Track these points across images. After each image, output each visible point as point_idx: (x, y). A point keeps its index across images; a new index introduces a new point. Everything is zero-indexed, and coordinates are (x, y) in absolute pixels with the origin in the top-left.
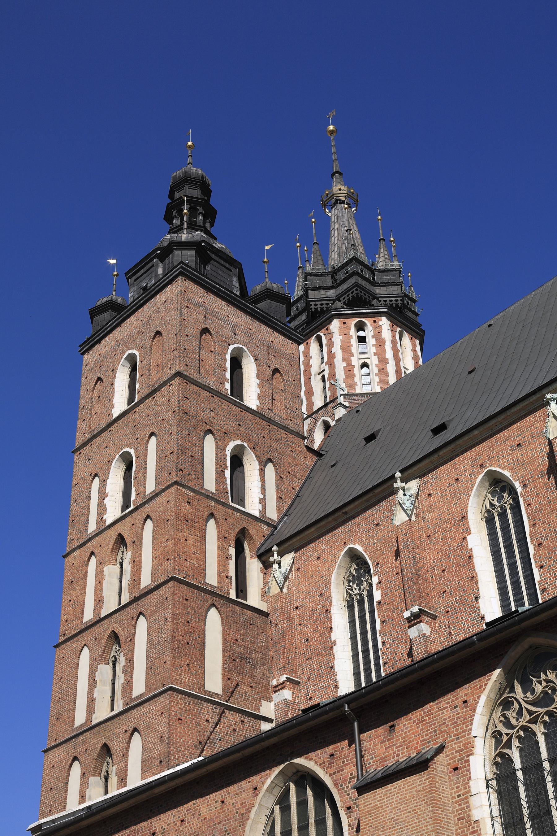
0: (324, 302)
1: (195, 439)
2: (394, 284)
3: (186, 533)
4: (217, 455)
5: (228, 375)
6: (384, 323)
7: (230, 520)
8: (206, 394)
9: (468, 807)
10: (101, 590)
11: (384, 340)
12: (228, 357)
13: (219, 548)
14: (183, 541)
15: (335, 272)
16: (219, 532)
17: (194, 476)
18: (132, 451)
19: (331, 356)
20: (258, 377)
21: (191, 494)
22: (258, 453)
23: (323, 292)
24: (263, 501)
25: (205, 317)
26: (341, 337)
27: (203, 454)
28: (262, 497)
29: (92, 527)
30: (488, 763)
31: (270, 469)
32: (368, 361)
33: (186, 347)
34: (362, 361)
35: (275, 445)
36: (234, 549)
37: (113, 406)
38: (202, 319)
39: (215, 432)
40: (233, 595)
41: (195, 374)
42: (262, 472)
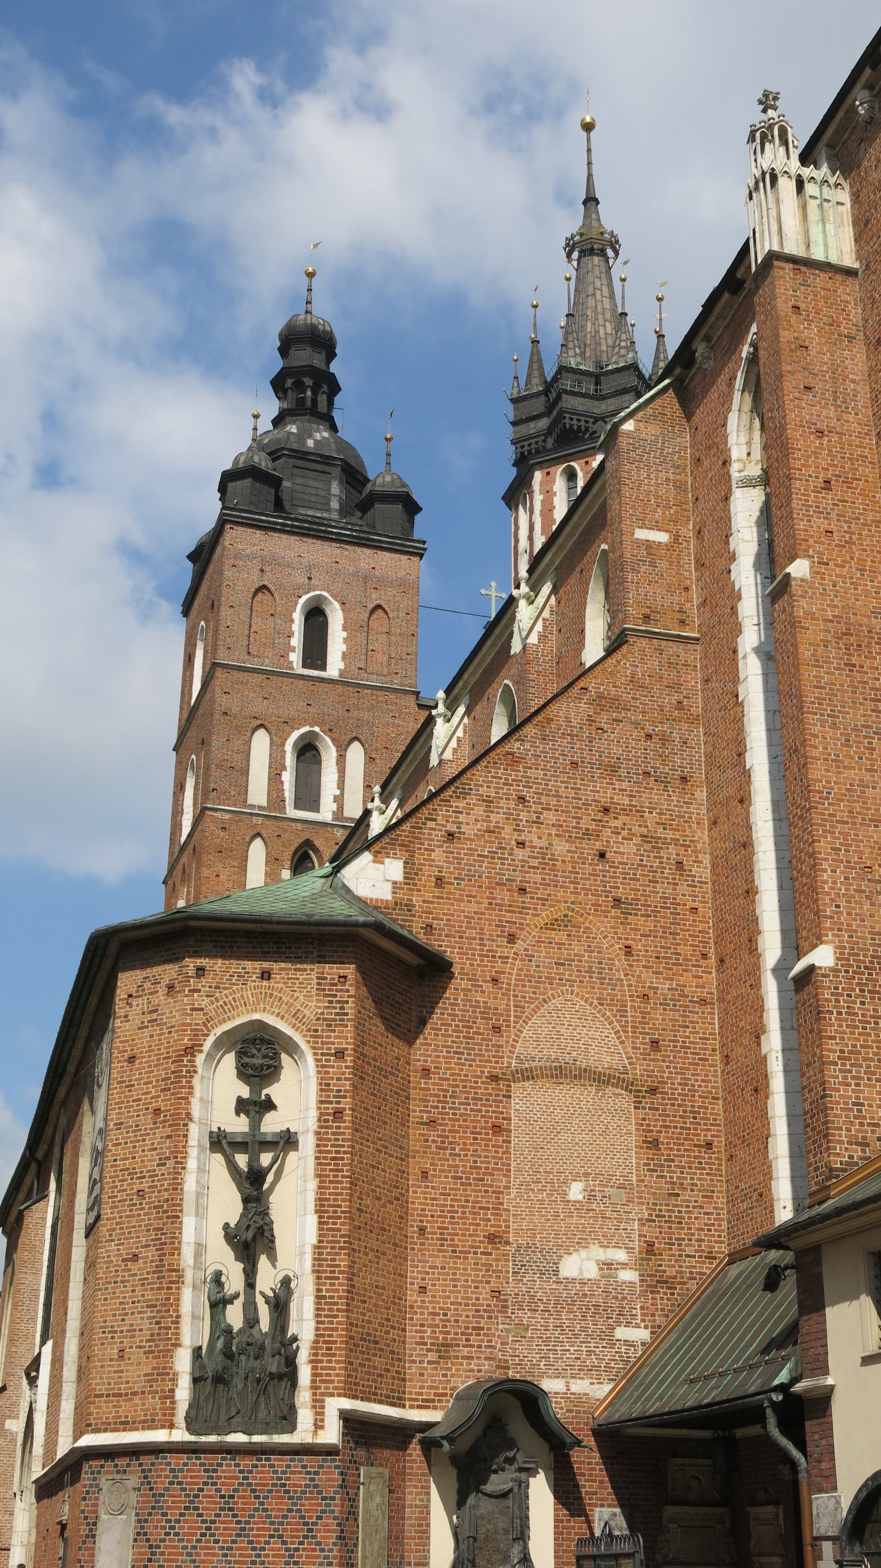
0: (533, 441)
1: (237, 743)
3: (219, 867)
4: (271, 755)
7: (286, 836)
8: (256, 679)
16: (268, 854)
17: (233, 793)
20: (345, 628)
21: (227, 816)
22: (335, 736)
23: (532, 425)
25: (262, 570)
27: (248, 761)
28: (338, 792)
35: (366, 716)
39: (269, 726)
42: (341, 759)
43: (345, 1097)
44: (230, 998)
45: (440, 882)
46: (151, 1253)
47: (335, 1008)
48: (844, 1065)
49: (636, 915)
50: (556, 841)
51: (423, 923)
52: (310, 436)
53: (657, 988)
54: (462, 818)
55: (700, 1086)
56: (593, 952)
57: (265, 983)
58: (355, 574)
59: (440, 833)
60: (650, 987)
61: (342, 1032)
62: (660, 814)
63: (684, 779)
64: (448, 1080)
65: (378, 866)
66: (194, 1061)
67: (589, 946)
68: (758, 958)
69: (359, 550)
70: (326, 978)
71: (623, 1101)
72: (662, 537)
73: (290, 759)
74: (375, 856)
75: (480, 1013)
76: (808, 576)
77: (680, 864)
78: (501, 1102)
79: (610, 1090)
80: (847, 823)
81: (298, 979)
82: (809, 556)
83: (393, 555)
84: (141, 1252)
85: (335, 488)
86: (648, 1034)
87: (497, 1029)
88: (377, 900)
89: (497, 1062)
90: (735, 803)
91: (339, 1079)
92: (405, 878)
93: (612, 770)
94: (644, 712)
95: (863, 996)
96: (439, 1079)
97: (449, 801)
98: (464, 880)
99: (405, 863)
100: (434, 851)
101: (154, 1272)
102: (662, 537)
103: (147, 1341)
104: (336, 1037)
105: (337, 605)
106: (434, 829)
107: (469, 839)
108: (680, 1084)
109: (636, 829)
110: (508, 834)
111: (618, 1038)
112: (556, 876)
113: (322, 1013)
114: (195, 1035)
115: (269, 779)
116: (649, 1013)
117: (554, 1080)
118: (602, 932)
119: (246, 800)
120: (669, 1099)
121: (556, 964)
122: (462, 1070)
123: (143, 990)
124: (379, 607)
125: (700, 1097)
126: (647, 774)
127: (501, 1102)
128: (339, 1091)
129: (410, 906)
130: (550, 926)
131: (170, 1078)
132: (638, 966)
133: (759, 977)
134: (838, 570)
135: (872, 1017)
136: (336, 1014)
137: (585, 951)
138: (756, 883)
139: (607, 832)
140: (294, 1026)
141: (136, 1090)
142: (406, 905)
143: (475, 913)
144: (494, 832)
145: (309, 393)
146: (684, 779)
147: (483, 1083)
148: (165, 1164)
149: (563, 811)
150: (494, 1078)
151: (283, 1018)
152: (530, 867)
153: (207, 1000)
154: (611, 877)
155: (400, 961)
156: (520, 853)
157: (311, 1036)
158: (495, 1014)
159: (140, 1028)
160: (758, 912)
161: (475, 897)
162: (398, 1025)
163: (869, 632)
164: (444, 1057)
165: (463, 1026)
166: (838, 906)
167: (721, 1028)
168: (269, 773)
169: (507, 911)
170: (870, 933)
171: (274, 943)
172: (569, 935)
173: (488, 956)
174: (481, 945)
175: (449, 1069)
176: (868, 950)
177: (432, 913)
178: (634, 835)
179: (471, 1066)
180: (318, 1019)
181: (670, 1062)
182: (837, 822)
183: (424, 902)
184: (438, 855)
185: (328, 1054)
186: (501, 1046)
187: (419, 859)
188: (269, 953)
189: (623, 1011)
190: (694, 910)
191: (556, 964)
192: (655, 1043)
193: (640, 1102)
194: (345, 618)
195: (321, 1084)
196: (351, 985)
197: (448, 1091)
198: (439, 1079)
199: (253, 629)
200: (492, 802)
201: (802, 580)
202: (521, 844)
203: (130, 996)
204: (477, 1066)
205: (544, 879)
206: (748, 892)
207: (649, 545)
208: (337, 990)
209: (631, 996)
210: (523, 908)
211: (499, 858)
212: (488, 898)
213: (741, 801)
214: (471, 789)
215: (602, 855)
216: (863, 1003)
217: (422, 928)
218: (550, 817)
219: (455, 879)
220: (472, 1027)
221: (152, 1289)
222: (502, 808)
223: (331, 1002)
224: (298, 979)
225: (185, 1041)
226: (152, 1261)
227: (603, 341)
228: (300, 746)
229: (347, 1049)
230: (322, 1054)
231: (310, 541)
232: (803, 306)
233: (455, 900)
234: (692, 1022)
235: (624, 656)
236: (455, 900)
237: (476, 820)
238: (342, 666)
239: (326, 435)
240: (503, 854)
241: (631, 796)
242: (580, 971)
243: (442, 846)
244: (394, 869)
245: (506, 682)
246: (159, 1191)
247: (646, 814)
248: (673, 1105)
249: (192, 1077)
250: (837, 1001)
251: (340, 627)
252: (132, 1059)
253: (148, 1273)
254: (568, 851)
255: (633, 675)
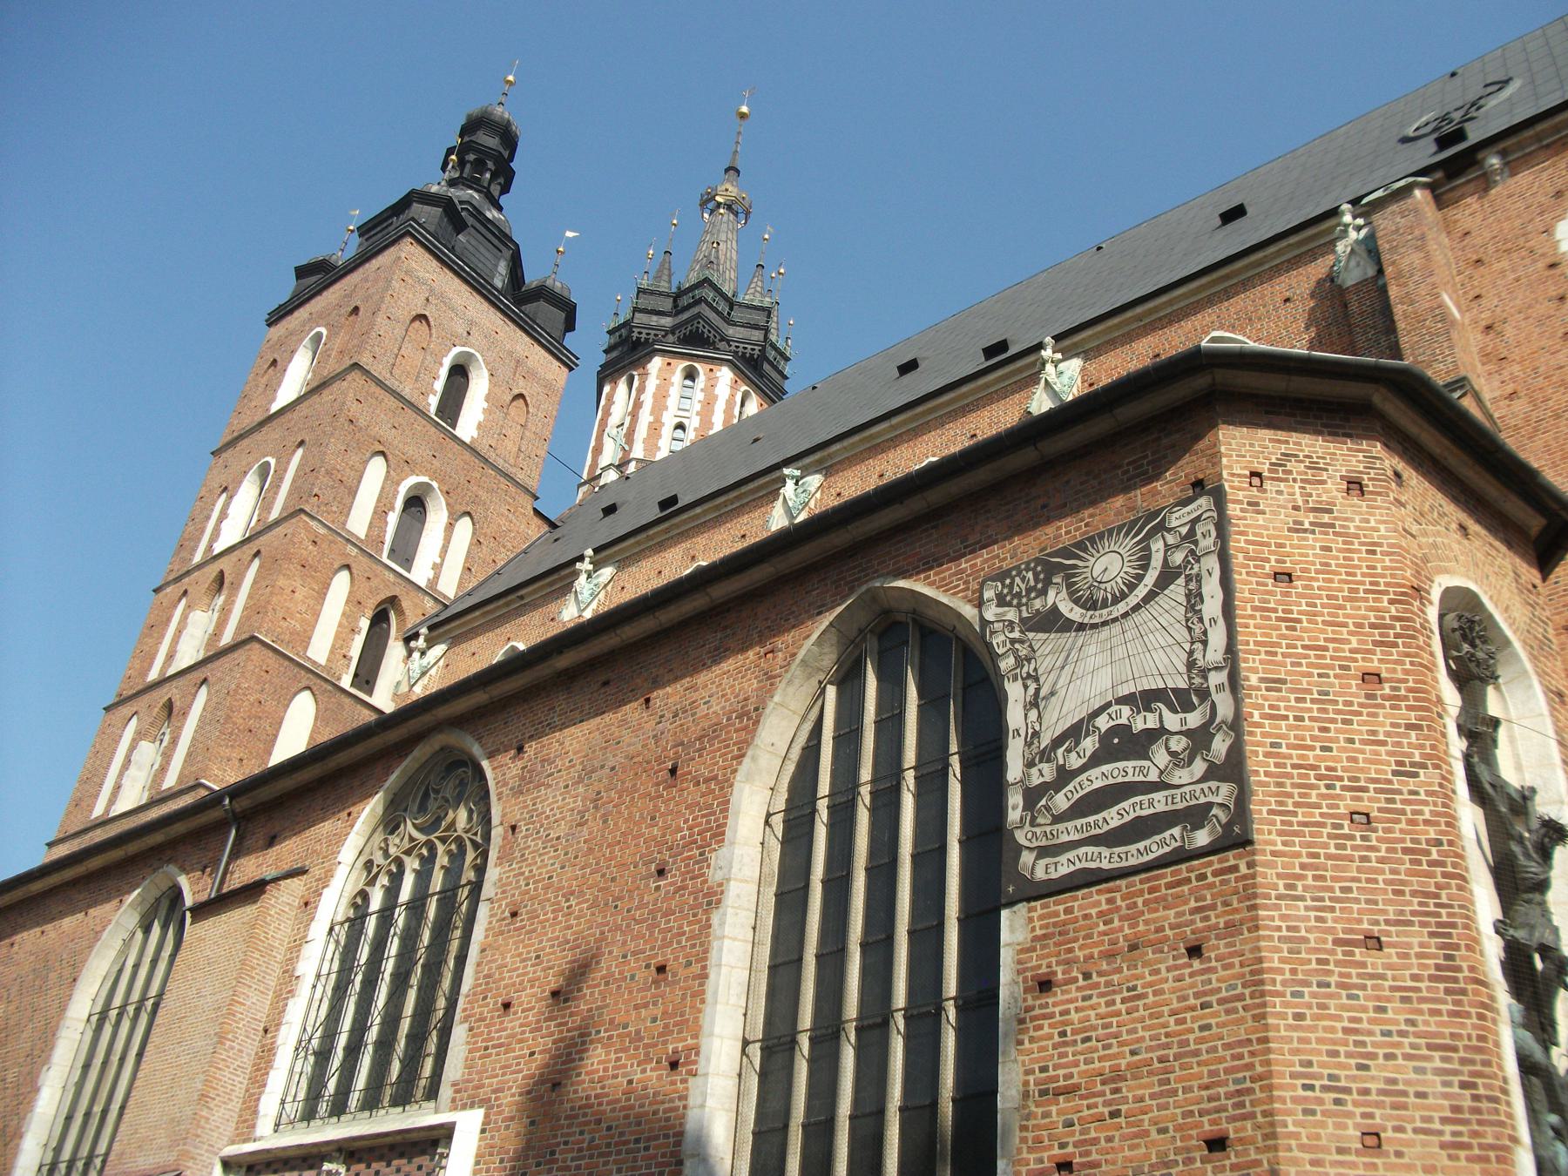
0: (653, 332)
1: (354, 459)
2: (756, 327)
3: (298, 584)
4: (383, 488)
5: (439, 385)
6: (725, 375)
7: (375, 582)
8: (392, 403)
9: (298, 957)
10: (177, 643)
11: (716, 398)
12: (447, 362)
13: (344, 614)
14: (288, 591)
15: (680, 293)
17: (334, 509)
18: (273, 461)
19: (638, 405)
20: (487, 399)
21: (322, 531)
23: (655, 318)
24: (437, 568)
26: (658, 382)
27: (359, 482)
28: (438, 561)
29: (198, 558)
30: (345, 901)
31: (464, 527)
32: (686, 422)
34: (679, 420)
35: (484, 495)
36: (368, 622)
37: (274, 399)
38: (421, 300)
39: (390, 457)
40: (346, 682)
41: (384, 372)
42: (450, 527)
46: (1416, 937)
58: (511, 353)
73: (399, 503)
83: (547, 355)
84: (1388, 934)
101: (1432, 978)
103: (1444, 1120)
105: (486, 373)
115: (375, 512)
119: (344, 524)
124: (521, 396)
145: (488, 175)
148: (1416, 775)
168: (376, 507)
199: (402, 352)
221: (1438, 1013)
226: (1419, 956)
228: (411, 494)
231: (478, 298)
246: (1411, 822)
253: (1415, 978)
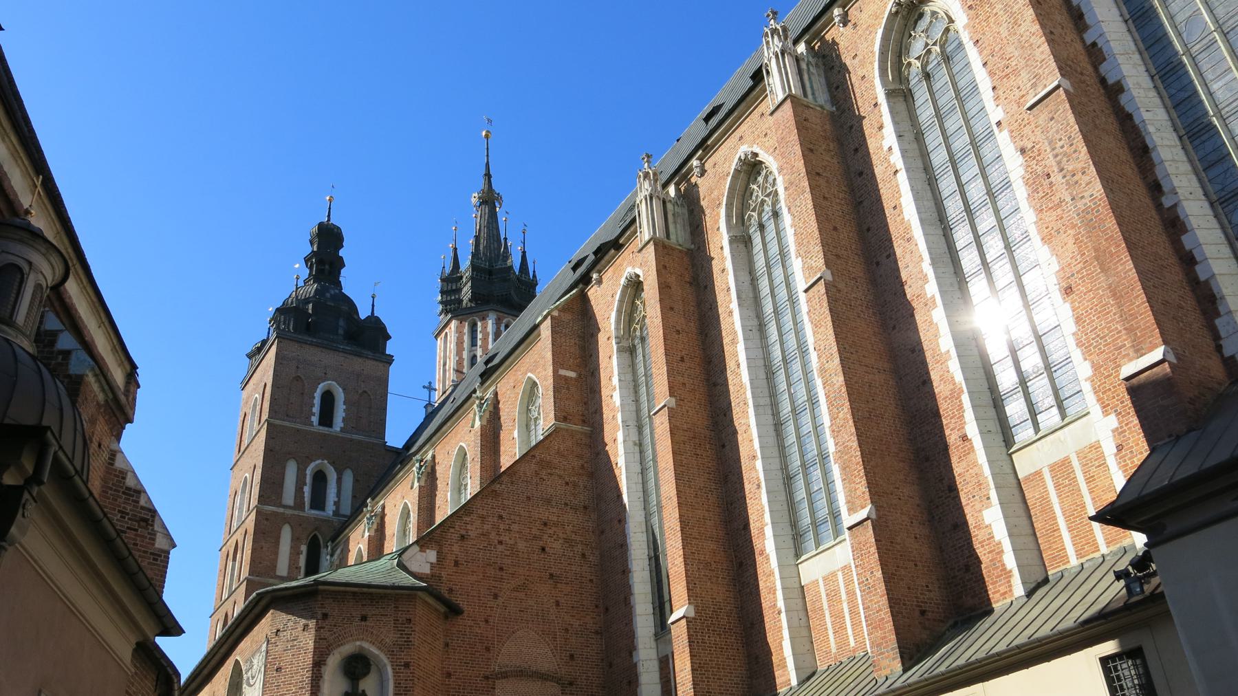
13: (291, 547)
17: (274, 498)
20: (345, 403)
27: (283, 479)
28: (336, 499)
33: (276, 397)
43: (410, 691)
44: (343, 632)
45: (456, 563)
47: (404, 638)
48: (701, 670)
49: (561, 583)
50: (518, 541)
51: (448, 587)
52: (328, 292)
53: (572, 625)
54: (469, 527)
55: (595, 680)
56: (539, 604)
57: (363, 623)
59: (457, 535)
60: (569, 624)
61: (408, 652)
62: (573, 526)
63: (585, 508)
64: (461, 679)
65: (424, 554)
66: (320, 670)
67: (537, 601)
68: (631, 609)
69: (355, 358)
70: (398, 620)
71: (554, 688)
72: (572, 374)
73: (309, 479)
74: (421, 548)
75: (479, 639)
76: (675, 406)
77: (583, 555)
78: (490, 691)
79: (548, 683)
80: (698, 539)
81: (382, 621)
82: (675, 396)
85: (341, 323)
86: (568, 651)
87: (488, 649)
88: (422, 574)
89: (487, 668)
90: (616, 522)
91: (406, 680)
92: (438, 561)
93: (548, 501)
94: (564, 470)
95: (709, 633)
96: (456, 678)
97: (461, 517)
98: (469, 562)
99: (438, 552)
100: (453, 545)
102: (572, 374)
104: (405, 655)
105: (341, 390)
106: (454, 533)
107: (472, 539)
108: (585, 679)
109: (561, 535)
110: (493, 535)
111: (553, 653)
112: (519, 560)
113: (397, 641)
114: (322, 655)
115: (296, 490)
116: (569, 639)
117: (519, 678)
118: (543, 593)
119: (280, 503)
120: (580, 688)
121: (520, 611)
122: (468, 673)
123: (288, 627)
124: (365, 392)
125: (596, 686)
126: (566, 504)
127: (490, 691)
128: (406, 687)
129: (440, 577)
130: (515, 590)
131: (305, 681)
132: (562, 612)
133: (632, 619)
134: (689, 403)
135: (714, 644)
136: (405, 641)
137: (535, 603)
138: (630, 567)
139: (545, 537)
140: (380, 649)
141: (281, 688)
142: (438, 577)
143: (476, 581)
144: (485, 535)
145: (327, 267)
146: (585, 508)
147: (480, 680)
149: (523, 524)
150: (487, 678)
151: (374, 644)
152: (505, 555)
153: (328, 633)
154: (548, 562)
155: (436, 610)
156: (500, 548)
157: (390, 655)
158: (486, 640)
159: (284, 650)
160: (631, 583)
161: (475, 572)
162: (435, 647)
163: (705, 437)
164: (459, 666)
165: (470, 648)
166: (695, 584)
167: (606, 647)
168: (296, 487)
169: (493, 580)
170: (711, 598)
171: (369, 599)
172: (526, 594)
173: (482, 606)
174: (479, 600)
175: (462, 672)
176: (710, 607)
177: (452, 581)
178: (560, 538)
179: (473, 670)
180: (394, 645)
181: (580, 667)
182: (694, 538)
183: (448, 575)
184: (456, 548)
185: (400, 666)
186: (490, 659)
187: (445, 550)
188: (365, 605)
189: (555, 638)
190: (591, 581)
191: (520, 611)
192: (572, 657)
193: (565, 690)
194: (345, 398)
195: (395, 683)
196: (414, 624)
197: (460, 685)
198: (456, 678)
200: (485, 518)
201: (672, 408)
202: (500, 542)
203: (278, 631)
204: (477, 671)
205: (512, 562)
206: (624, 571)
207: (566, 378)
208: (405, 627)
209: (559, 629)
210: (502, 579)
211: (488, 550)
212: (483, 573)
213: (620, 521)
214: (473, 511)
215: (543, 549)
216: (709, 637)
217: (447, 590)
218: (515, 527)
219: (465, 562)
220: (474, 648)
222: (490, 521)
223: (401, 634)
224: (382, 621)
225: (315, 658)
227: (493, 252)
228: (316, 471)
229: (410, 662)
230: (397, 665)
232: (668, 265)
233: (464, 573)
234: (591, 644)
235: (554, 439)
236: (464, 573)
237: (477, 528)
238: (342, 425)
239: (337, 291)
240: (491, 548)
241: (558, 516)
242: (532, 615)
243: (457, 543)
244: (432, 555)
245: (461, 444)
247: (566, 527)
248: (581, 691)
249: (319, 680)
250: (697, 635)
251: (342, 404)
252: (279, 669)
254: (525, 547)
255: (559, 448)
